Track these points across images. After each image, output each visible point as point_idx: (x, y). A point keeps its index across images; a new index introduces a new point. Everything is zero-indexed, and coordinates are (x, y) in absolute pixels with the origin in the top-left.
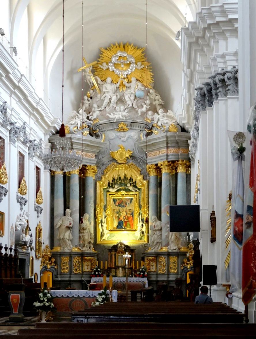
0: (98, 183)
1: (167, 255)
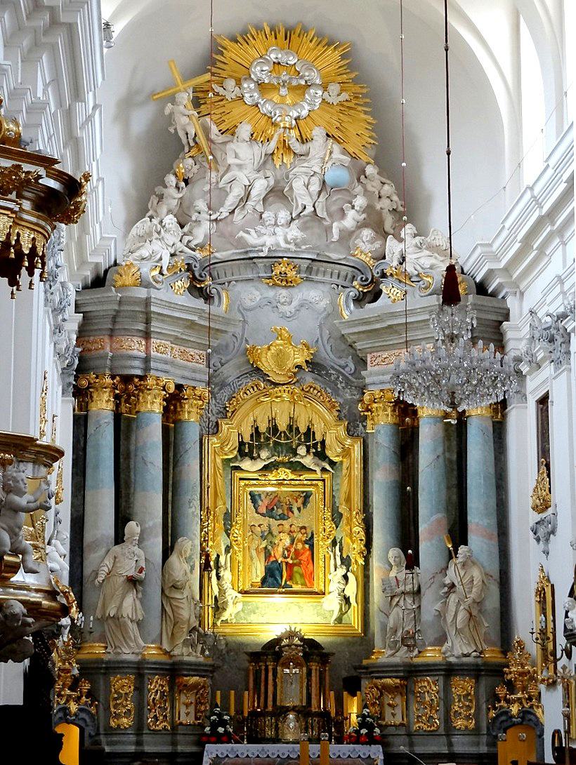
1: (443, 673)
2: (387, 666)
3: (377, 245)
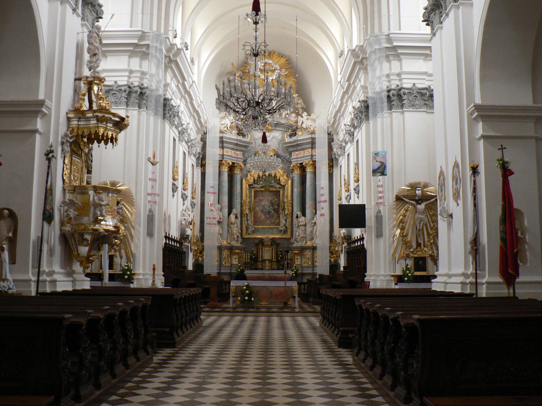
0: (244, 180)
3: (296, 119)
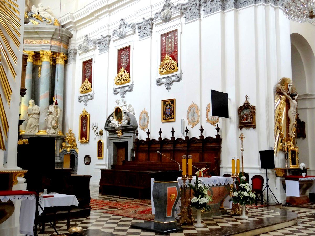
2: (28, 135)
